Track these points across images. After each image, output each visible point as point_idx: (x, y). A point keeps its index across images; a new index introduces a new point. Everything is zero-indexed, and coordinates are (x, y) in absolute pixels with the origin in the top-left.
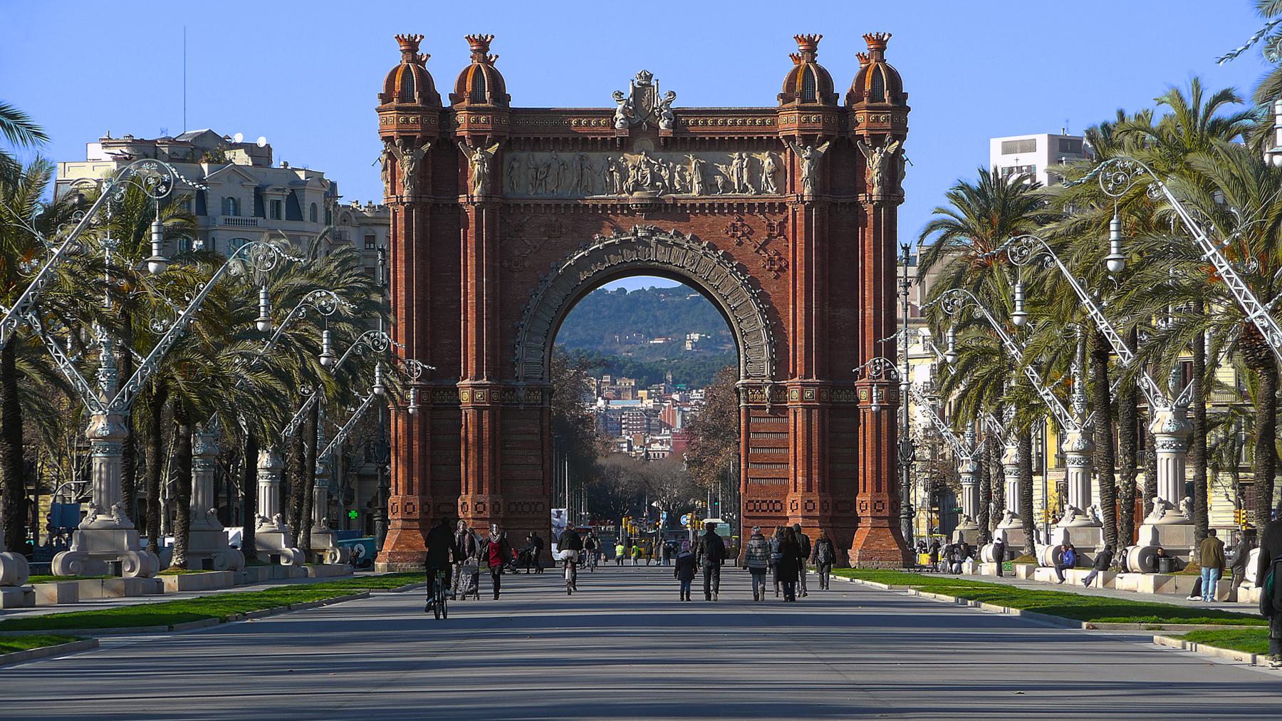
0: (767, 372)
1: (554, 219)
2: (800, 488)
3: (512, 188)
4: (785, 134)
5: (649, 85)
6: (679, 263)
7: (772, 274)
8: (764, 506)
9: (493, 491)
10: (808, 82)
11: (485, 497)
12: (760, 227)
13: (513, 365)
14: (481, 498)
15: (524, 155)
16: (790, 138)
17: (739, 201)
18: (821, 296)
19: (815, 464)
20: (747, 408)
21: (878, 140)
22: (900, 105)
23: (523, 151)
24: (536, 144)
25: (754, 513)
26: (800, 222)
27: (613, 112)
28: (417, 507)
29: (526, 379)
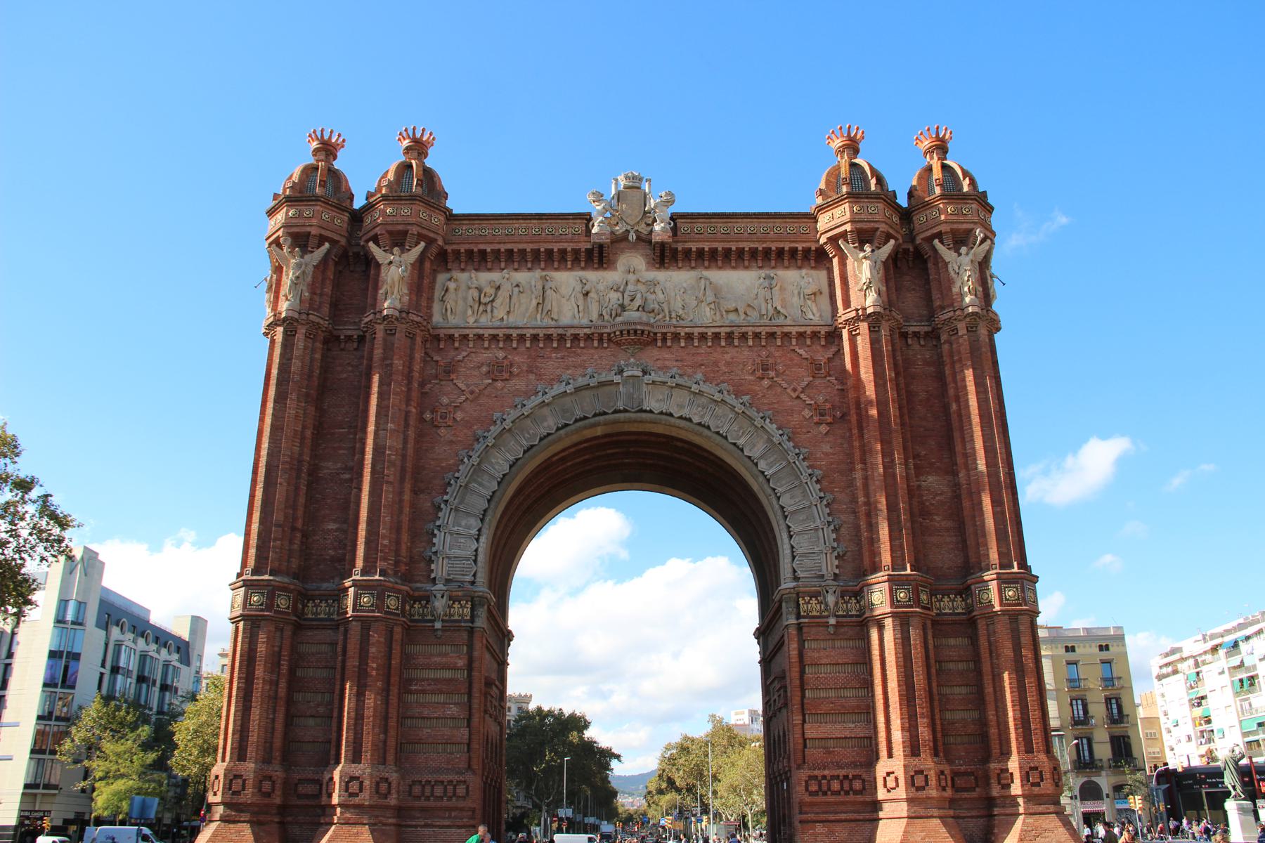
1: (501, 354)
2: (898, 749)
3: (445, 316)
6: (685, 412)
7: (823, 429)
9: (381, 758)
11: (363, 769)
12: (800, 366)
13: (431, 561)
14: (357, 770)
16: (843, 235)
17: (768, 329)
20: (800, 627)
21: (961, 239)
22: (981, 200)
23: (463, 270)
24: (480, 259)
29: (448, 581)
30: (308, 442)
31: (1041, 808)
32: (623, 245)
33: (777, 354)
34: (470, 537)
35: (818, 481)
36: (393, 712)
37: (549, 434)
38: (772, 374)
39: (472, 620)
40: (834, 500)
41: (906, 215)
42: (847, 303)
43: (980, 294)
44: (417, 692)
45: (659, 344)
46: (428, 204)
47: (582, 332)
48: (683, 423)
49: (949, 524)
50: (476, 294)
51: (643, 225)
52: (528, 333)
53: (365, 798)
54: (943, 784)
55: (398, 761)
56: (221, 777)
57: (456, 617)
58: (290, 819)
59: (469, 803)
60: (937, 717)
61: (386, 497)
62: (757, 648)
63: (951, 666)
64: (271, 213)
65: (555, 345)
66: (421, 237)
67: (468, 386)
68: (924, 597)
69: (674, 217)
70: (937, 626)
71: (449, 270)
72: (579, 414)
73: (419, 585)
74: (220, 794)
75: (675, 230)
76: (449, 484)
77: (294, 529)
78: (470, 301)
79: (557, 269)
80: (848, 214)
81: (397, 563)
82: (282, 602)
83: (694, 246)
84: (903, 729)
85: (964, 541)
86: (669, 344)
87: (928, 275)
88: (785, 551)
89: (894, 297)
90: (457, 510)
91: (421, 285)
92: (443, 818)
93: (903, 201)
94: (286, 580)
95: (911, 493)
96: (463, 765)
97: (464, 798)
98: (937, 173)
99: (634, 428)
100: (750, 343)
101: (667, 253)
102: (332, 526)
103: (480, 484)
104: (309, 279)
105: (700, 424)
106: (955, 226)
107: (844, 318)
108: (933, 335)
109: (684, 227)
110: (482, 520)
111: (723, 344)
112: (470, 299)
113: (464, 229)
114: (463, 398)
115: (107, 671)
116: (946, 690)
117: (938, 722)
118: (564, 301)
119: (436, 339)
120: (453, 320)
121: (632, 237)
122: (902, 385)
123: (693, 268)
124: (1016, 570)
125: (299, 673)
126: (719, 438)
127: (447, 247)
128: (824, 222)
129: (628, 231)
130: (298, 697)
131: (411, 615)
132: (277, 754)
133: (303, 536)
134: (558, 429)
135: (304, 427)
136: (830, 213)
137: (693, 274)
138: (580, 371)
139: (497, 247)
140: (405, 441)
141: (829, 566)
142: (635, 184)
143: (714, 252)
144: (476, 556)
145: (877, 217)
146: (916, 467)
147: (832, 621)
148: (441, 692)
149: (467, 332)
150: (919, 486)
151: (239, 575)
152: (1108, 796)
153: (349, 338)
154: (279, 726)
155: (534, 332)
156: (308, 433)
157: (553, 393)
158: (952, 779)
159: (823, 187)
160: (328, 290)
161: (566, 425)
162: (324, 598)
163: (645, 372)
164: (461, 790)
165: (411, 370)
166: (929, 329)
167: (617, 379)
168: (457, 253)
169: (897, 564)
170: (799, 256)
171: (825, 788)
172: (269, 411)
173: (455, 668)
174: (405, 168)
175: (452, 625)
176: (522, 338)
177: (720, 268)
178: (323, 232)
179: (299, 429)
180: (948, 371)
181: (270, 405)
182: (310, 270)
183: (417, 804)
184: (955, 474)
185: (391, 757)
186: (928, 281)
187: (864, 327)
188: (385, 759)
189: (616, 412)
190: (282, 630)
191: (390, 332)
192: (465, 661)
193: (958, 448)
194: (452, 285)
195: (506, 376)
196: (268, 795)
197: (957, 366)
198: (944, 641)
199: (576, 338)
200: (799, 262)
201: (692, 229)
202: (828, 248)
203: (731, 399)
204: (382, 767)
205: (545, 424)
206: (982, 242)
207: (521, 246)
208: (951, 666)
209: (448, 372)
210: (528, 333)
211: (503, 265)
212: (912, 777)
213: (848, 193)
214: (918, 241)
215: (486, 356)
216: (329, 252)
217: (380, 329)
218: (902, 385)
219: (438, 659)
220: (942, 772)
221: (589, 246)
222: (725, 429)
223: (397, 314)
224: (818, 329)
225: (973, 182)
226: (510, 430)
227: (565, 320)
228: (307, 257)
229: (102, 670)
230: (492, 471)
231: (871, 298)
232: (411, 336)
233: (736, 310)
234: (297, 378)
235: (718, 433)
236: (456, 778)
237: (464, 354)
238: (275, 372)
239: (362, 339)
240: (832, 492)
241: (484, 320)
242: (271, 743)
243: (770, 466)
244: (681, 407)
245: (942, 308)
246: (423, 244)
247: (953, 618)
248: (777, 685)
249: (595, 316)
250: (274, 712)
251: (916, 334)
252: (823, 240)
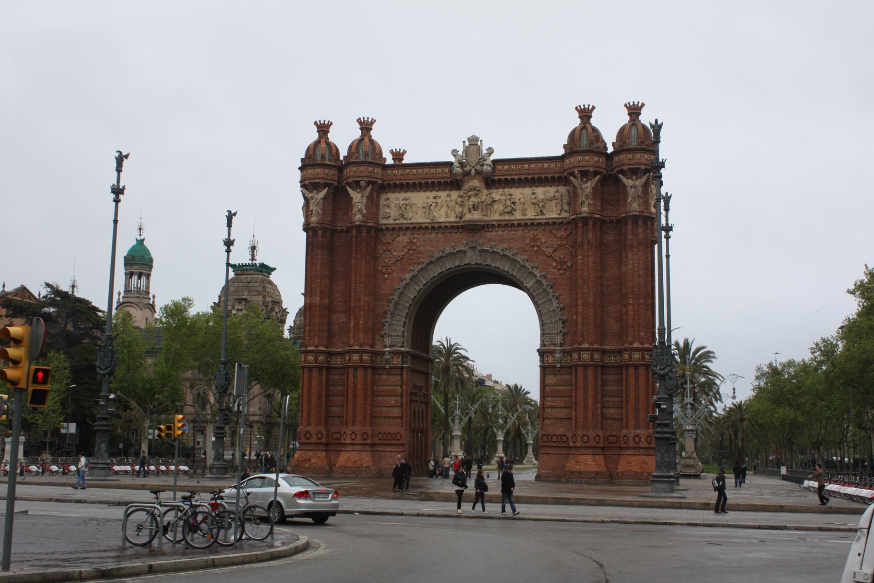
6: (497, 265)
7: (562, 272)
8: (554, 439)
10: (584, 138)
13: (383, 337)
21: (634, 172)
25: (548, 444)
35: (557, 298)
38: (538, 243)
41: (610, 157)
66: (368, 183)
69: (495, 162)
75: (494, 168)
83: (503, 178)
91: (373, 203)
93: (610, 149)
101: (490, 181)
120: (391, 221)
141: (559, 339)
147: (558, 365)
164: (398, 437)
168: (389, 184)
174: (361, 140)
187: (580, 224)
199: (446, 227)
217: (354, 232)
232: (368, 232)
251: (611, 221)
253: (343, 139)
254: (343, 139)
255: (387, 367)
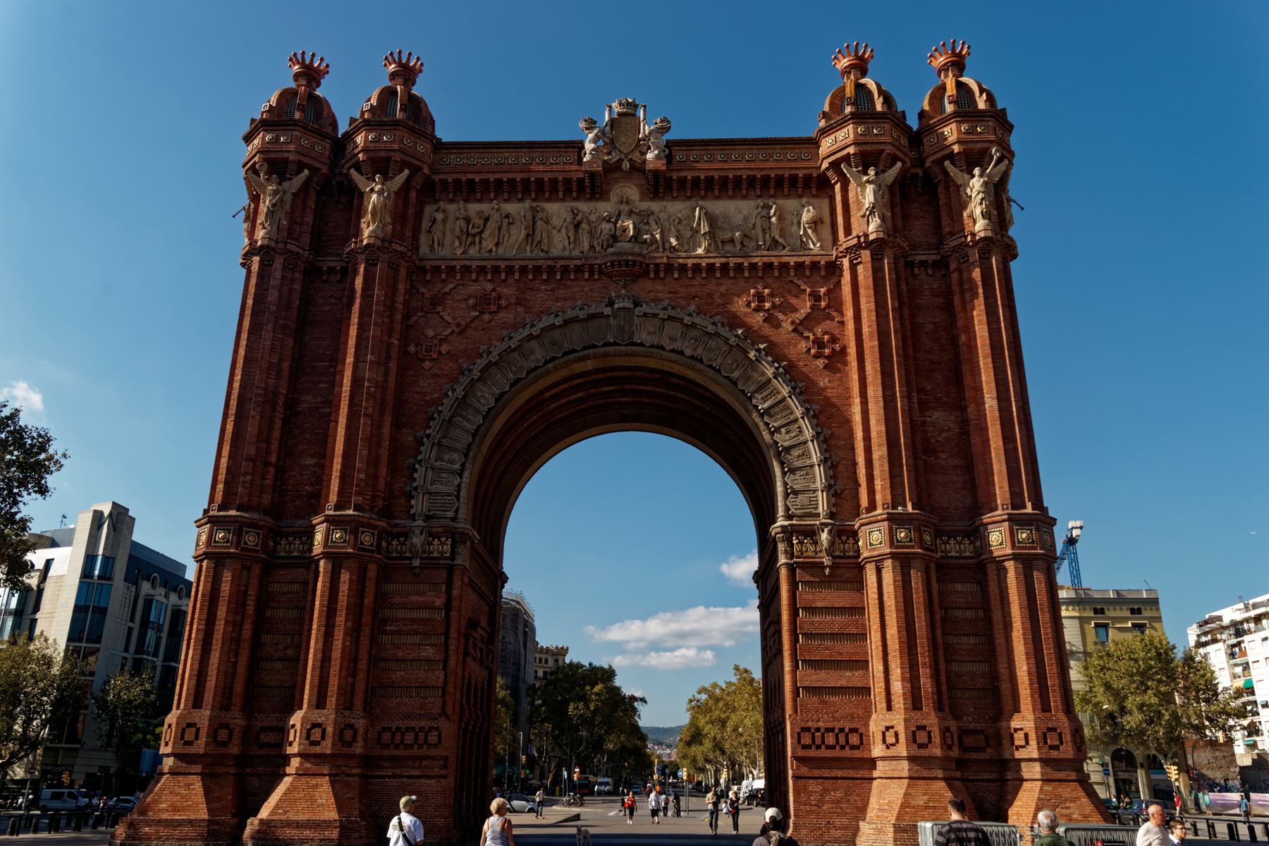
0: (822, 508)
1: (489, 286)
3: (432, 247)
4: (831, 159)
5: (634, 115)
7: (821, 363)
8: (830, 739)
9: (346, 703)
15: (451, 208)
16: (846, 158)
17: (766, 260)
18: (907, 382)
19: (923, 657)
20: (792, 569)
21: (973, 159)
22: (999, 119)
23: (452, 201)
24: (469, 190)
25: (812, 753)
26: (864, 273)
27: (579, 146)
28: (204, 732)
29: (428, 518)
30: (286, 374)
31: (1062, 775)
32: (616, 175)
33: (775, 285)
34: (452, 472)
36: (363, 655)
37: (536, 368)
39: (452, 558)
40: (832, 436)
41: (916, 139)
42: (848, 231)
43: (995, 219)
44: (392, 633)
45: (652, 275)
46: (412, 130)
47: (572, 264)
48: (674, 356)
49: (957, 462)
50: (462, 223)
51: (637, 154)
52: (517, 264)
53: (327, 747)
54: (949, 742)
55: (368, 709)
56: (174, 726)
57: (435, 555)
58: (249, 770)
59: (440, 752)
60: (942, 667)
61: (364, 431)
62: (757, 593)
63: (958, 613)
64: (248, 138)
65: (545, 277)
67: (454, 319)
68: (927, 538)
69: (670, 145)
70: (941, 571)
71: (437, 201)
72: (567, 347)
73: (398, 521)
74: (171, 744)
75: (669, 158)
76: (433, 419)
77: (267, 464)
78: (458, 232)
79: (549, 200)
80: (852, 136)
81: (374, 498)
82: (250, 539)
83: (689, 175)
84: (903, 680)
85: (973, 480)
86: (662, 275)
87: (938, 201)
88: (779, 489)
89: (899, 223)
90: (439, 444)
91: (406, 215)
92: (413, 768)
94: (255, 516)
95: (914, 428)
96: (436, 710)
97: (436, 745)
98: (951, 89)
99: (625, 362)
100: (747, 274)
102: (310, 461)
103: (465, 418)
104: (288, 207)
105: (692, 357)
106: (970, 145)
107: (844, 246)
108: (942, 264)
109: (679, 156)
110: (466, 455)
111: (718, 275)
112: (458, 229)
113: (453, 159)
114: (449, 331)
115: (136, 626)
116: (952, 640)
117: (943, 673)
118: (555, 232)
119: (421, 272)
120: (442, 253)
121: (626, 165)
122: (907, 316)
123: (689, 198)
124: (1029, 510)
125: (269, 613)
126: (711, 372)
127: (434, 177)
128: (826, 145)
129: (621, 160)
130: (266, 639)
131: (388, 552)
132: (237, 700)
133: (277, 472)
134: (546, 362)
135: (281, 360)
136: (832, 137)
137: (688, 203)
138: (569, 304)
139: (485, 176)
140: (386, 374)
142: (630, 111)
143: (710, 180)
144: (459, 491)
145: (883, 139)
146: (920, 402)
148: (417, 633)
149: (455, 263)
150: (924, 422)
151: (206, 511)
152: (1142, 765)
153: (332, 270)
154: (241, 670)
155: (524, 263)
156: (286, 366)
157: (541, 325)
158: (960, 737)
159: (826, 108)
160: (309, 219)
161: (554, 359)
162: (298, 535)
163: (636, 304)
164: (433, 738)
165: (394, 302)
166: (939, 257)
167: (607, 311)
168: (444, 183)
169: (897, 500)
170: (800, 184)
171: (818, 741)
172: (243, 343)
173: (432, 608)
174: (388, 95)
175: (430, 563)
176: (510, 270)
177: (717, 198)
178: (302, 158)
179: (275, 360)
180: (957, 300)
181: (244, 336)
182: (288, 197)
183: (386, 752)
184: (963, 409)
185: (358, 702)
186: (937, 208)
187: (866, 255)
188: (352, 703)
189: (607, 344)
190: (249, 569)
191: (371, 264)
192: (444, 600)
193: (968, 381)
194: (439, 216)
195: (493, 308)
196: (224, 744)
197: (967, 296)
198: (950, 586)
199: (565, 270)
200: (800, 190)
201: (688, 156)
202: (830, 174)
203: (724, 332)
204: (347, 713)
205: (533, 357)
206: (999, 161)
207: (511, 176)
208: (958, 613)
209: (435, 305)
210: (517, 264)
211: (492, 195)
212: (914, 733)
213: (851, 113)
214: (928, 164)
215: (473, 288)
216: (308, 180)
218: (907, 316)
219: (415, 598)
220: (947, 729)
221: (581, 175)
222: (719, 362)
223: (379, 243)
224: (818, 259)
225: (991, 99)
226: (496, 363)
227: (555, 252)
228: (286, 185)
229: (131, 624)
230: (478, 405)
231: (874, 223)
232: (394, 268)
233: (732, 241)
234: (273, 308)
235: (710, 366)
236: (426, 724)
237: (452, 286)
238: (250, 302)
239: (344, 271)
240: (830, 427)
241: (473, 252)
242: (231, 689)
243: (764, 400)
244: (673, 339)
245: (952, 234)
246: (406, 172)
247: (961, 561)
248: (772, 629)
249: (586, 246)
250: (237, 655)
251: (923, 264)
252: (825, 165)
253: (349, 98)
254: (349, 98)
255: (416, 563)
